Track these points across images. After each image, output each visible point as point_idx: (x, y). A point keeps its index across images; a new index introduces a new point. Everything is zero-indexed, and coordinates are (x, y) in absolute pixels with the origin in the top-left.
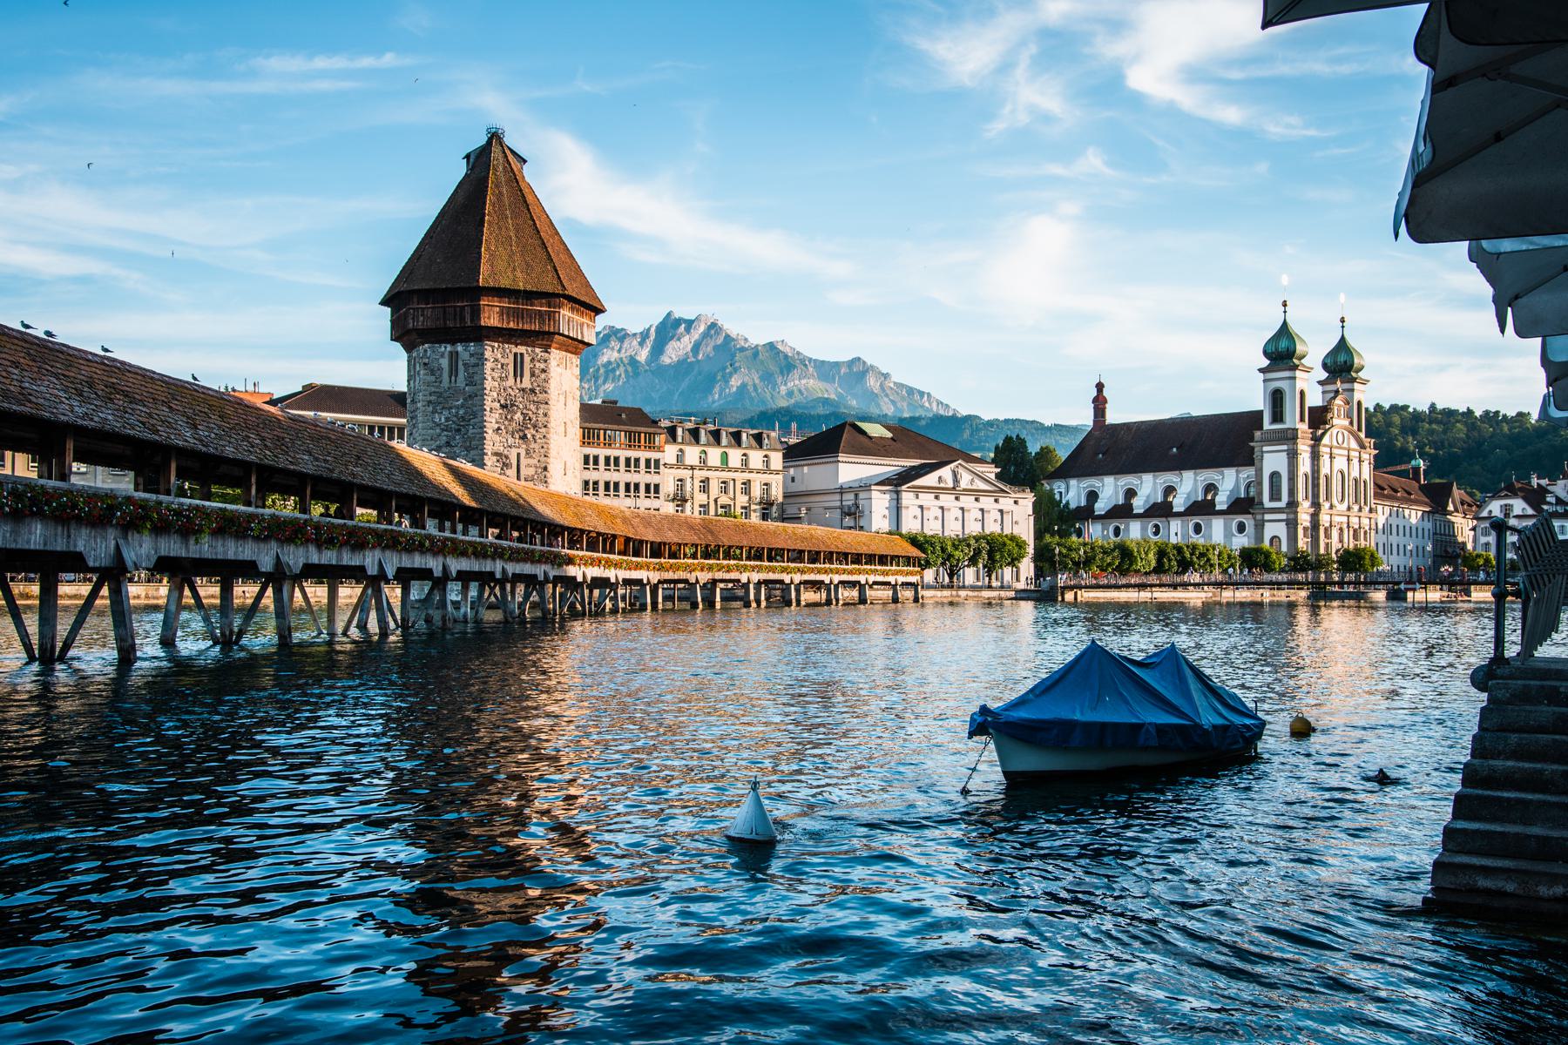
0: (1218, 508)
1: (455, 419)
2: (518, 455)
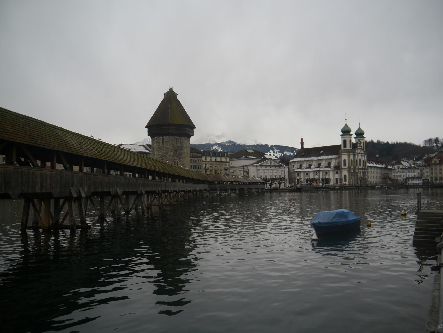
1: (163, 154)
2: (178, 161)
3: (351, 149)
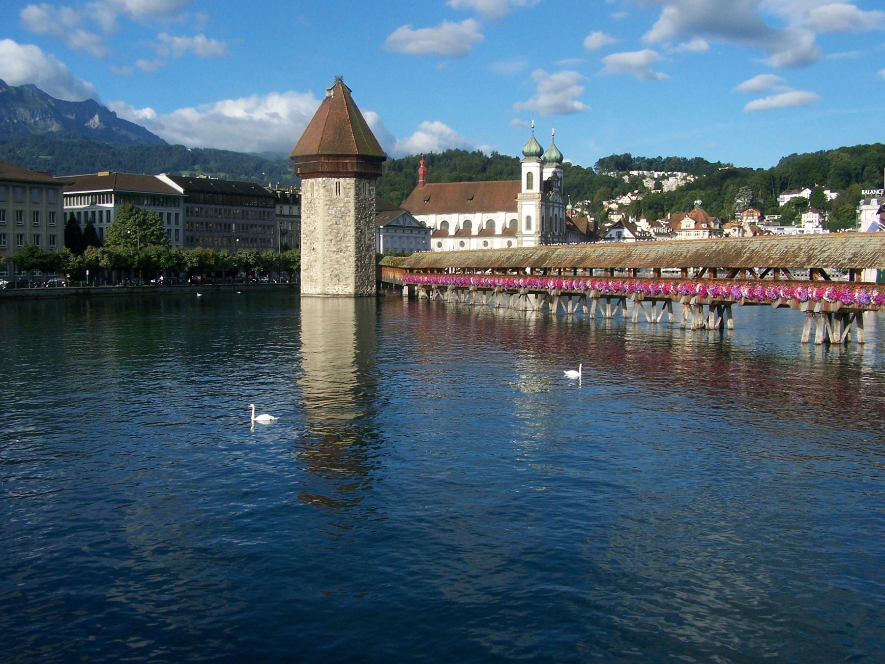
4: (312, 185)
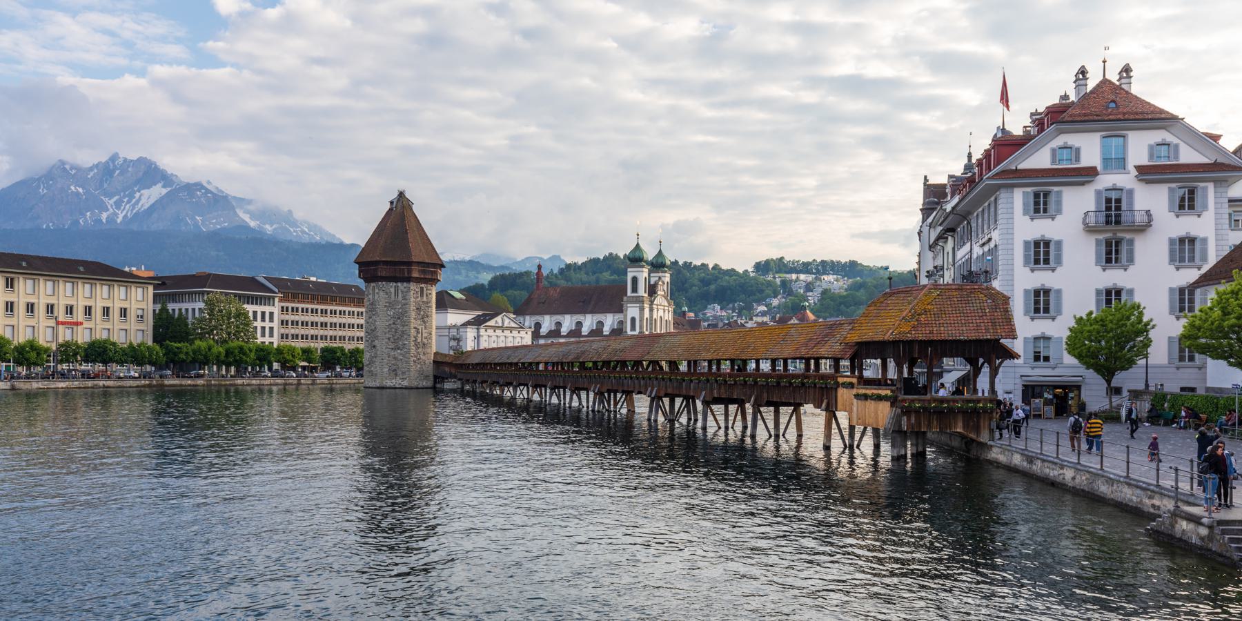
0: (604, 333)
3: (646, 295)
4: (374, 287)
